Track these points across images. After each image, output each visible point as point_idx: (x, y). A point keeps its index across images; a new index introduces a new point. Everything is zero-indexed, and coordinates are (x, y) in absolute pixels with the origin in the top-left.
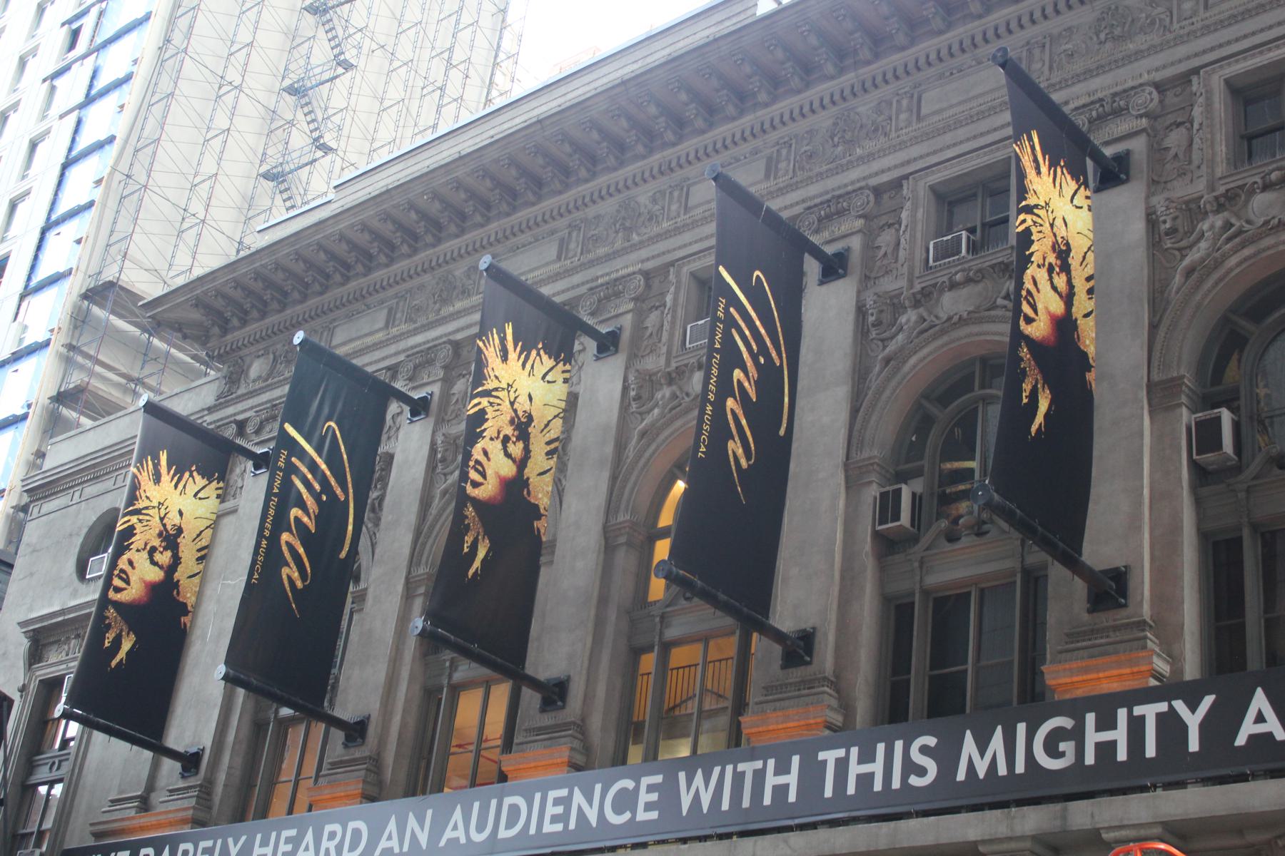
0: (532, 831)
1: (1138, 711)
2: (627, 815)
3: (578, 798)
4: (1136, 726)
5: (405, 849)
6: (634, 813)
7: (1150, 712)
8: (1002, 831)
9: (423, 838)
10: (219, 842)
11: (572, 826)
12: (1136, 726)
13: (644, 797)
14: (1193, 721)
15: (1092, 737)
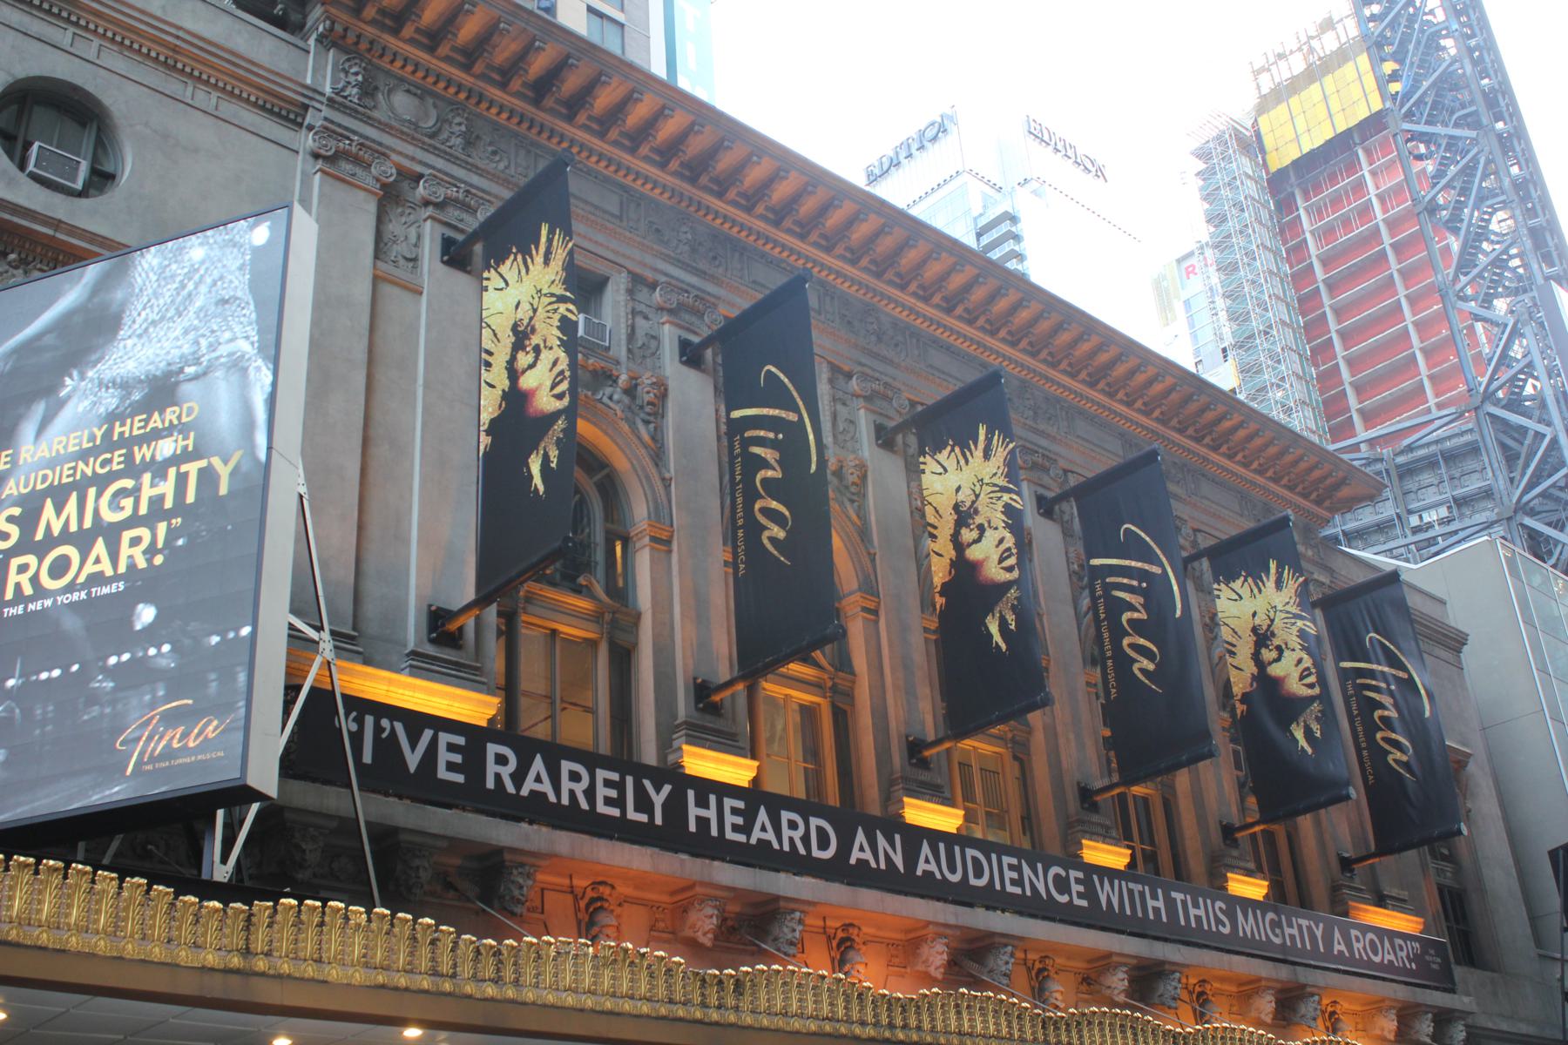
0: (998, 887)
1: (1301, 921)
2: (1064, 899)
3: (1026, 870)
4: (1300, 927)
5: (883, 866)
6: (1070, 895)
7: (1304, 923)
8: (1274, 975)
9: (898, 860)
10: (629, 780)
11: (1028, 893)
12: (1300, 927)
13: (1076, 888)
14: (1319, 933)
15: (1288, 931)
